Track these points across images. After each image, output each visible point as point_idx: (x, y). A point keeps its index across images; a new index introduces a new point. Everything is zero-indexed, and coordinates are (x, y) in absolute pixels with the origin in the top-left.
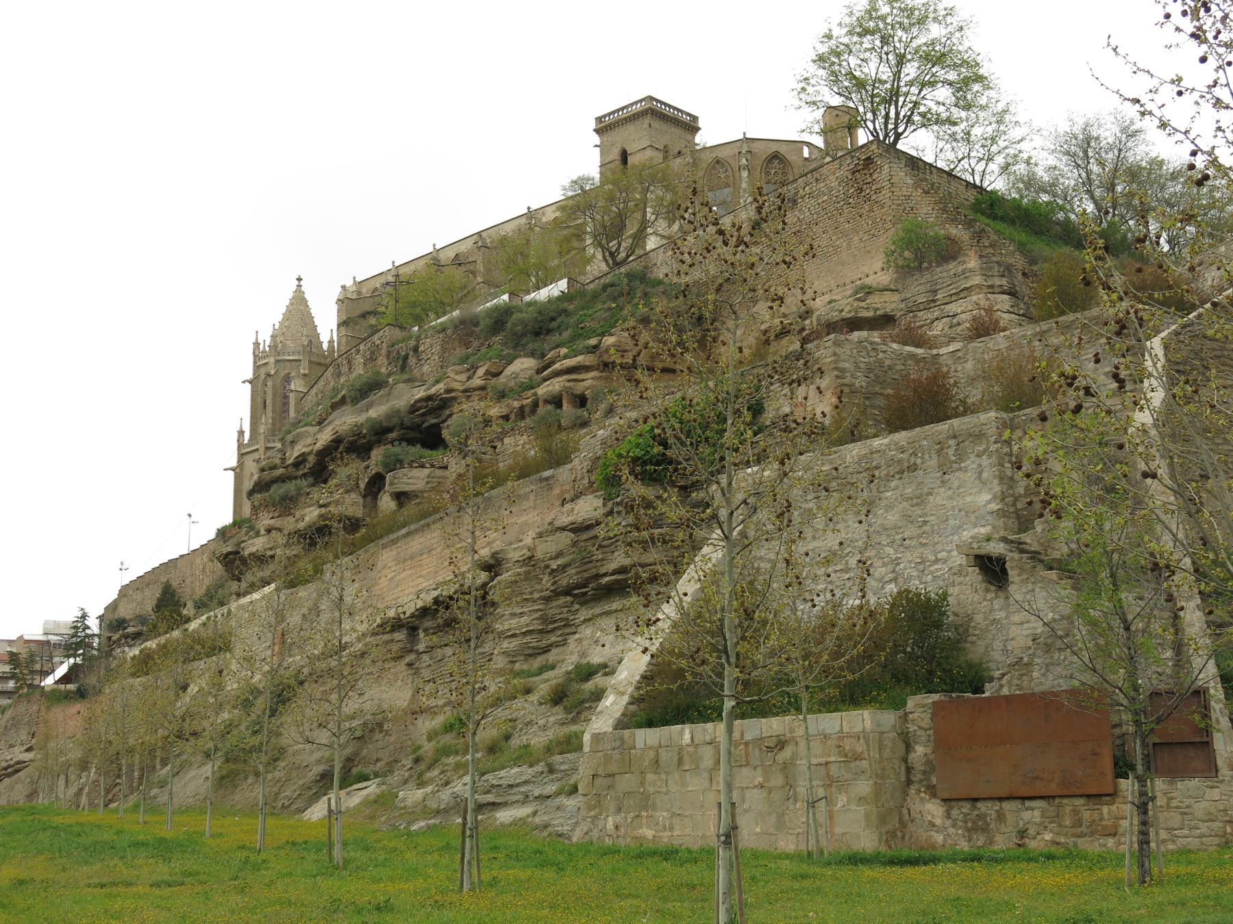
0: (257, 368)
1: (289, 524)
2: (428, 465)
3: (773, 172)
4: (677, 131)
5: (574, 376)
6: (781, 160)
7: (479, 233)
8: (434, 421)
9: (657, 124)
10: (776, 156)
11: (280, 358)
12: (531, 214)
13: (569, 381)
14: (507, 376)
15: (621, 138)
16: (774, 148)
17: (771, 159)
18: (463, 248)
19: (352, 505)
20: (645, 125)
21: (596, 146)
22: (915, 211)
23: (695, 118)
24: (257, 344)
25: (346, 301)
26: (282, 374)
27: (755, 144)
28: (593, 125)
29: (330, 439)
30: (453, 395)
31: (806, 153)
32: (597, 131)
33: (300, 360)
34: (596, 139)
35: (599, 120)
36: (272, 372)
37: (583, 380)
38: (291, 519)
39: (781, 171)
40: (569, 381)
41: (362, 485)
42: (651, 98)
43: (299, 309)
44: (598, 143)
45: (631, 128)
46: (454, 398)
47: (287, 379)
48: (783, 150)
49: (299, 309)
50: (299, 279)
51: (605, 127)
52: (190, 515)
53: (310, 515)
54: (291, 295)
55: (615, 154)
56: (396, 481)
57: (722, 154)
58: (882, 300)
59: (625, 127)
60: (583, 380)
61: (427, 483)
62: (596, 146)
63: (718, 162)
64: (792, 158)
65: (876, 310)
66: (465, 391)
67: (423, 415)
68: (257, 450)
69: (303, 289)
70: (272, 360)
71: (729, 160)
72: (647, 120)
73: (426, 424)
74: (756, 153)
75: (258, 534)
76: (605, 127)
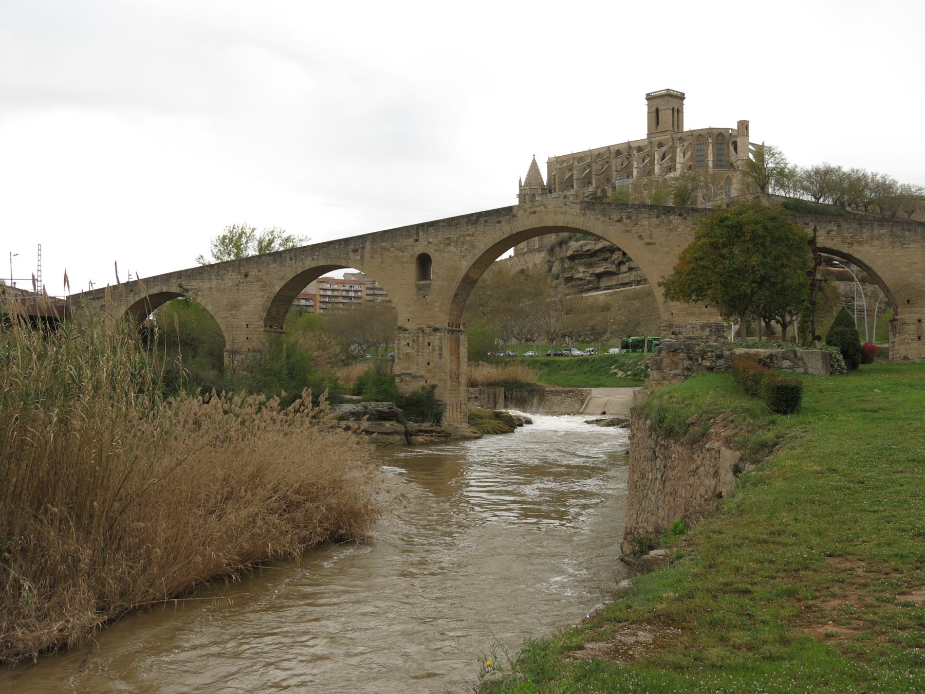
0: (521, 190)
1: (591, 271)
4: (677, 100)
7: (608, 147)
9: (670, 99)
10: (720, 134)
12: (629, 143)
16: (720, 131)
18: (602, 151)
19: (612, 268)
23: (683, 94)
24: (520, 181)
27: (713, 130)
28: (645, 97)
31: (730, 132)
32: (647, 99)
34: (646, 102)
35: (648, 95)
38: (592, 269)
41: (616, 263)
42: (669, 90)
43: (534, 167)
45: (660, 100)
47: (534, 195)
48: (723, 132)
49: (534, 167)
51: (650, 98)
53: (599, 270)
54: (531, 162)
55: (654, 109)
57: (702, 133)
63: (700, 135)
64: (726, 134)
70: (528, 188)
72: (667, 98)
75: (579, 272)
76: (650, 98)
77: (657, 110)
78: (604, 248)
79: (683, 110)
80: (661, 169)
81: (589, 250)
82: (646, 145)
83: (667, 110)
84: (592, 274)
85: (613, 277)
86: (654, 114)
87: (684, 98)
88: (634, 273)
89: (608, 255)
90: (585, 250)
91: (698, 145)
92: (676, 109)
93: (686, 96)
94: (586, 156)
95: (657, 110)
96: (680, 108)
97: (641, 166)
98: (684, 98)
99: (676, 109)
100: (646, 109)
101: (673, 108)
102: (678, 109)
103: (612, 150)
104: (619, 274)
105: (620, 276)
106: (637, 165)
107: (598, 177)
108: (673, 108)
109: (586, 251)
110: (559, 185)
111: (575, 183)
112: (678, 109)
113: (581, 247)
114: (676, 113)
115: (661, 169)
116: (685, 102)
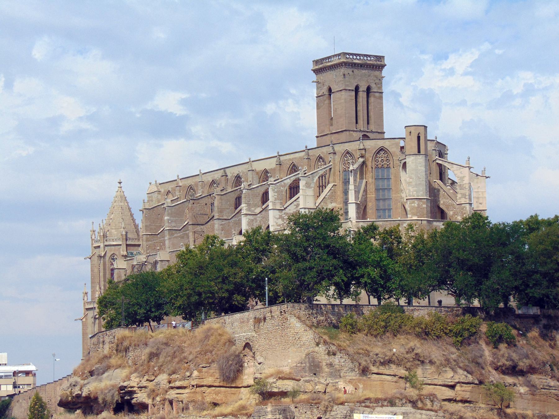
3: (380, 160)
6: (386, 151)
9: (348, 71)
15: (330, 77)
17: (379, 152)
20: (341, 74)
22: (300, 340)
23: (380, 58)
25: (144, 211)
28: (311, 66)
33: (120, 245)
34: (314, 77)
35: (316, 62)
39: (385, 159)
44: (315, 80)
58: (282, 384)
59: (329, 72)
62: (313, 82)
63: (348, 153)
65: (279, 389)
66: (138, 388)
69: (123, 189)
70: (102, 245)
71: (353, 153)
72: (343, 70)
74: (369, 148)
79: (380, 88)
80: (281, 217)
82: (274, 170)
83: (343, 93)
87: (381, 67)
92: (363, 88)
93: (386, 61)
96: (373, 86)
97: (258, 210)
98: (383, 66)
99: (363, 88)
101: (357, 89)
102: (368, 90)
103: (229, 175)
106: (249, 209)
107: (199, 228)
108: (357, 89)
110: (147, 240)
112: (368, 90)
114: (362, 95)
115: (281, 217)
116: (385, 72)
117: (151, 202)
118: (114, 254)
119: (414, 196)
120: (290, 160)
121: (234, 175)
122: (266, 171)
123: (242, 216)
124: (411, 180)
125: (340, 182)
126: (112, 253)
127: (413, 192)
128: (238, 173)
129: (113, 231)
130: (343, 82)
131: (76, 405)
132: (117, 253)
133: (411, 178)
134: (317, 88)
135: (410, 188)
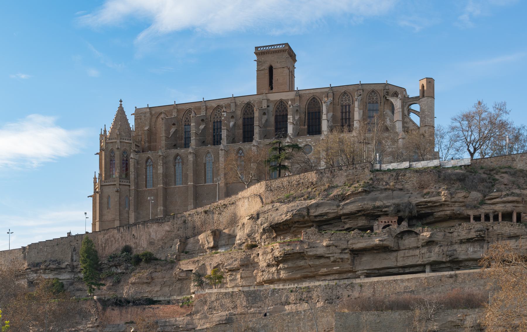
2: (443, 231)
5: (516, 204)
8: (430, 211)
11: (122, 140)
13: (513, 206)
14: (472, 199)
15: (270, 60)
21: (255, 60)
26: (122, 149)
29: (356, 209)
30: (447, 203)
33: (131, 143)
34: (255, 58)
36: (119, 147)
37: (518, 207)
40: (513, 206)
46: (448, 204)
50: (121, 101)
52: (86, 213)
56: (433, 236)
60: (518, 207)
61: (443, 238)
62: (255, 60)
67: (421, 208)
68: (115, 185)
69: (123, 106)
70: (118, 141)
73: (423, 212)
77: (271, 69)
78: (359, 211)
81: (326, 214)
84: (345, 249)
85: (384, 255)
86: (267, 71)
88: (437, 249)
89: (362, 222)
90: (316, 214)
91: (370, 103)
94: (199, 109)
95: (271, 69)
100: (254, 66)
104: (398, 250)
105: (401, 254)
109: (316, 216)
111: (193, 138)
113: (308, 208)
117: (139, 120)
118: (125, 149)
119: (431, 124)
120: (311, 93)
121: (243, 102)
122: (282, 101)
123: (288, 124)
124: (429, 113)
125: (366, 110)
126: (124, 148)
127: (430, 121)
128: (248, 101)
129: (123, 133)
130: (285, 62)
131: (305, 223)
132: (128, 149)
133: (429, 112)
134: (258, 65)
135: (428, 119)
